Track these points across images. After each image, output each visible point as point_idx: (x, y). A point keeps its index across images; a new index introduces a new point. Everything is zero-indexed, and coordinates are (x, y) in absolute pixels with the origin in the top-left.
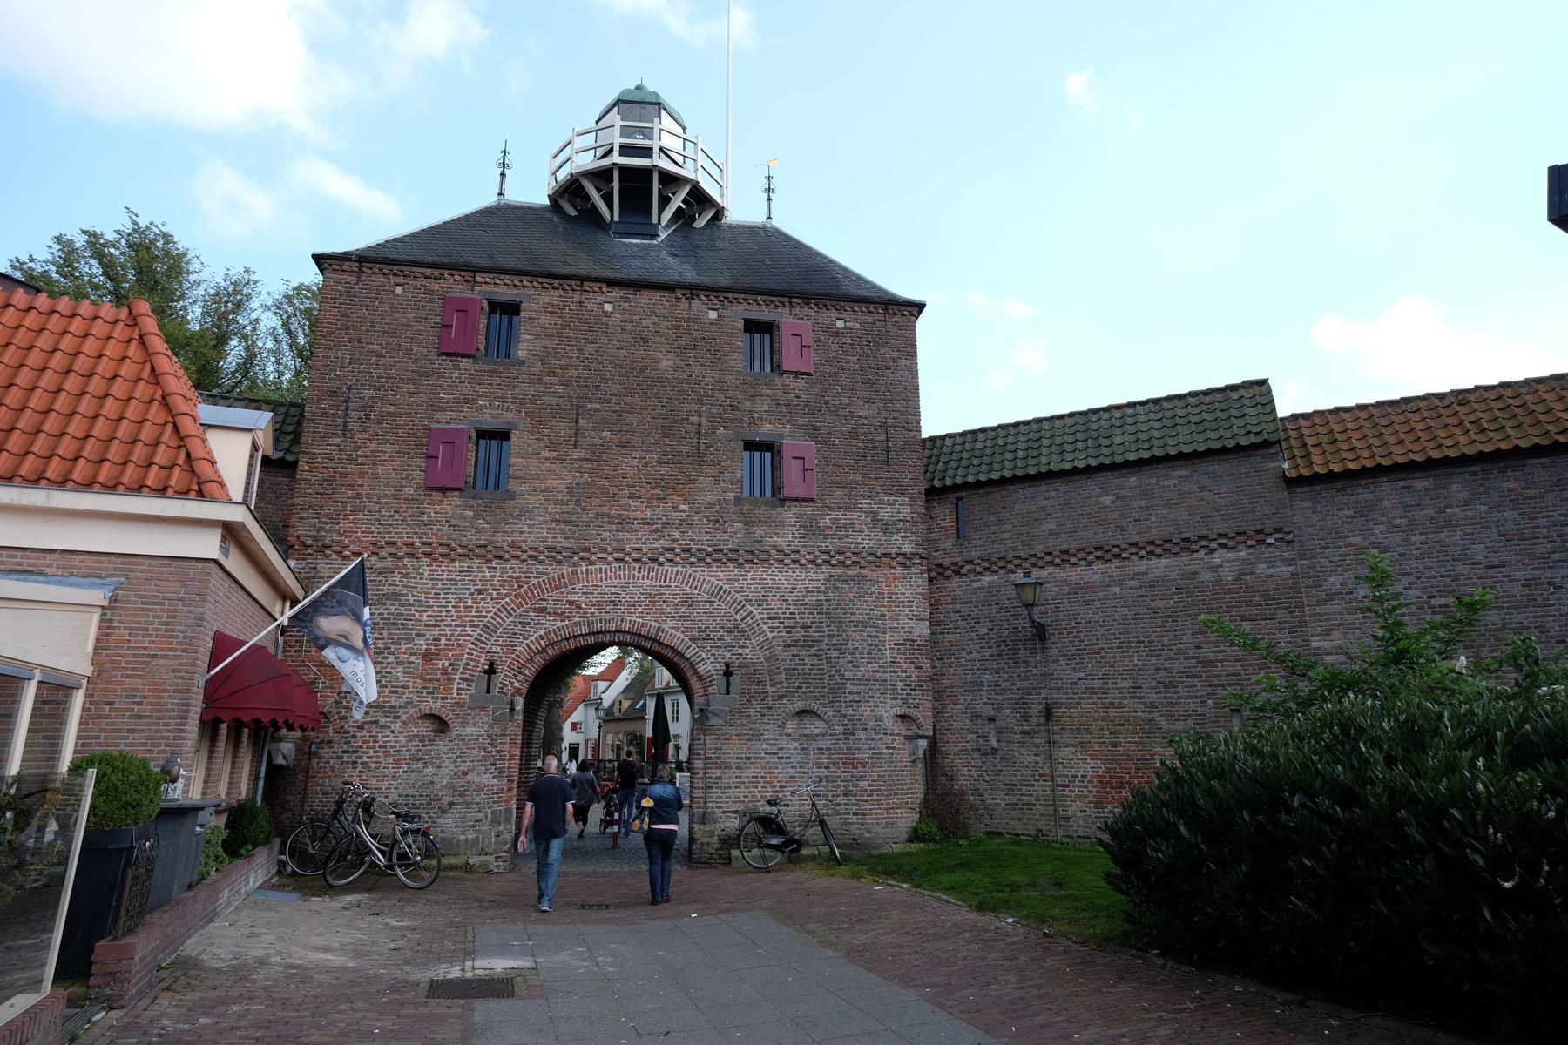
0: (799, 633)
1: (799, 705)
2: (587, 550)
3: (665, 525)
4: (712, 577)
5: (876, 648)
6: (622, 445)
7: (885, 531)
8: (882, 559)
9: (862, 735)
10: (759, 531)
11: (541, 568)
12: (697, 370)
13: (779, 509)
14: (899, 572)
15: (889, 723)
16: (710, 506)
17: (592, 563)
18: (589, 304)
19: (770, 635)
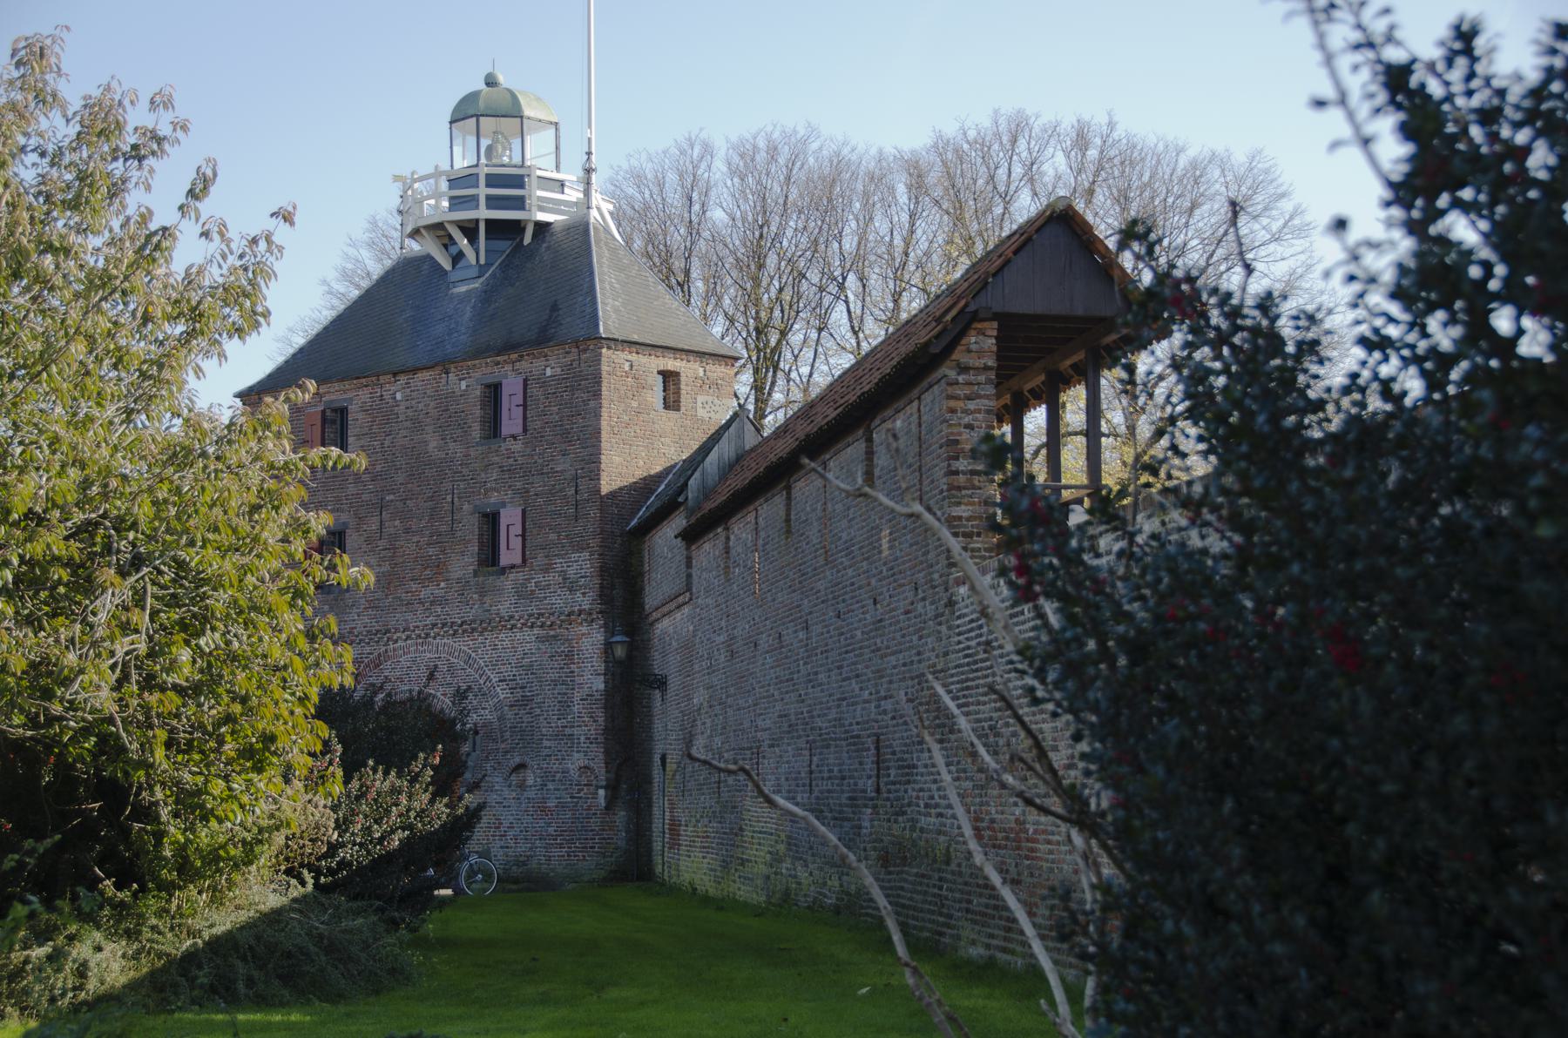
0: (519, 693)
1: (517, 760)
2: (388, 631)
3: (432, 603)
4: (462, 644)
5: (565, 705)
6: (407, 531)
7: (571, 590)
8: (570, 617)
9: (551, 786)
10: (487, 600)
11: (368, 649)
12: (452, 445)
13: (502, 578)
14: (584, 629)
15: (574, 774)
16: (459, 581)
17: (396, 641)
18: (387, 396)
19: (502, 697)
